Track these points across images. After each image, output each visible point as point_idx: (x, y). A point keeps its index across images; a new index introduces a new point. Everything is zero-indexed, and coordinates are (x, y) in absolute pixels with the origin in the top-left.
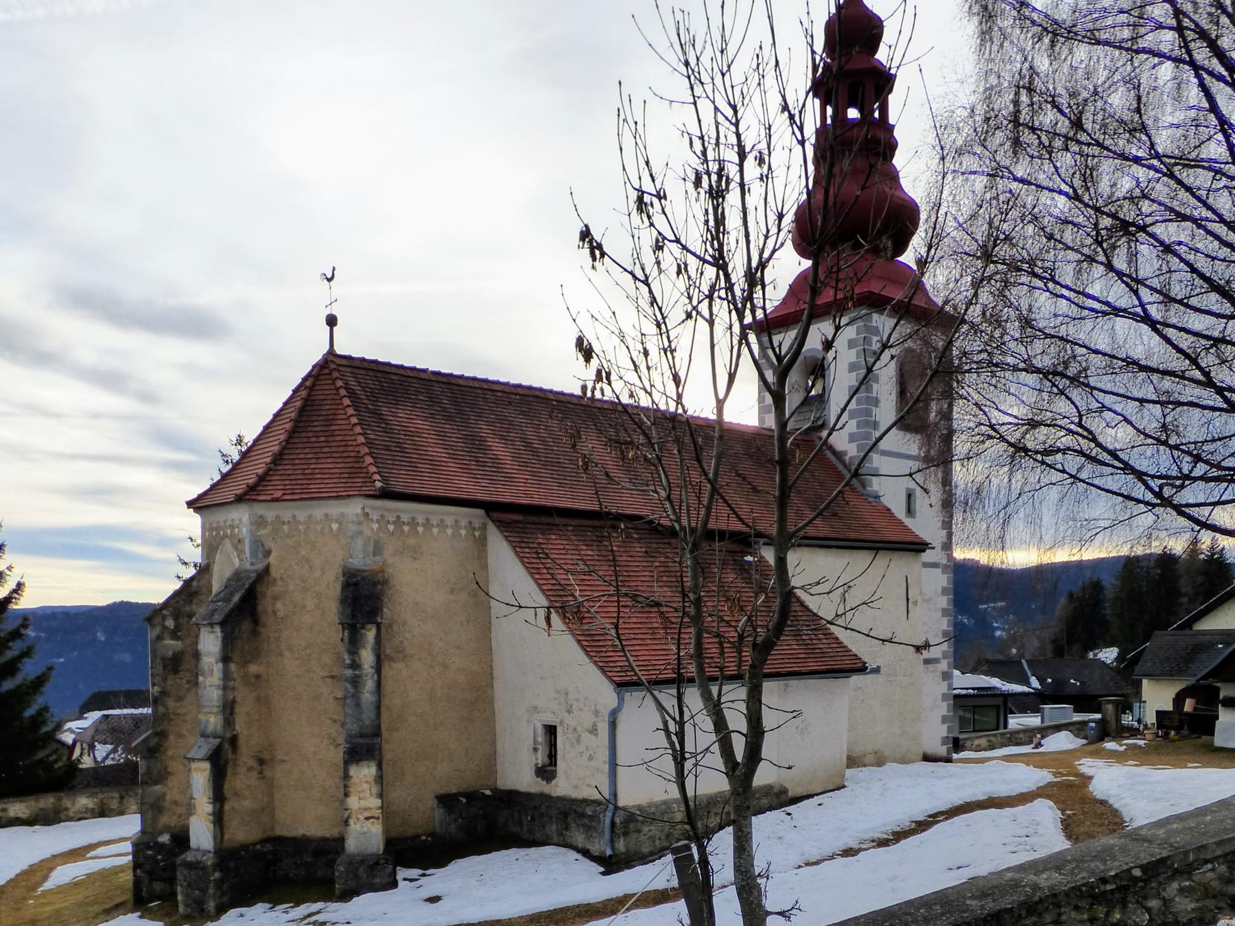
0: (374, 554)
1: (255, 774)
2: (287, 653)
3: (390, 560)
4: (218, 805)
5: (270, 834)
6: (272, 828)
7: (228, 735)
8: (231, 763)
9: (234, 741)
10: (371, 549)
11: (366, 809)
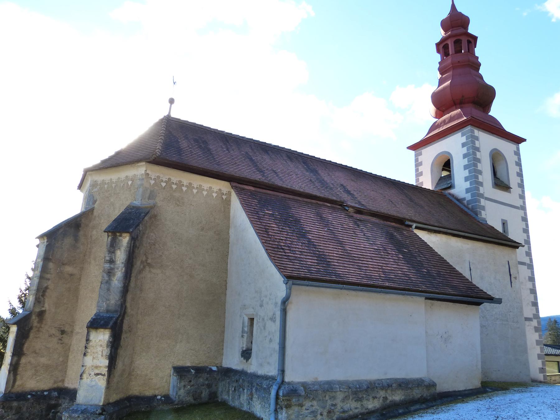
0: (149, 199)
1: (55, 340)
2: (93, 262)
3: (159, 204)
4: (15, 359)
5: (60, 385)
6: (63, 381)
7: (37, 310)
8: (34, 330)
9: (41, 314)
10: (147, 195)
11: (97, 367)
